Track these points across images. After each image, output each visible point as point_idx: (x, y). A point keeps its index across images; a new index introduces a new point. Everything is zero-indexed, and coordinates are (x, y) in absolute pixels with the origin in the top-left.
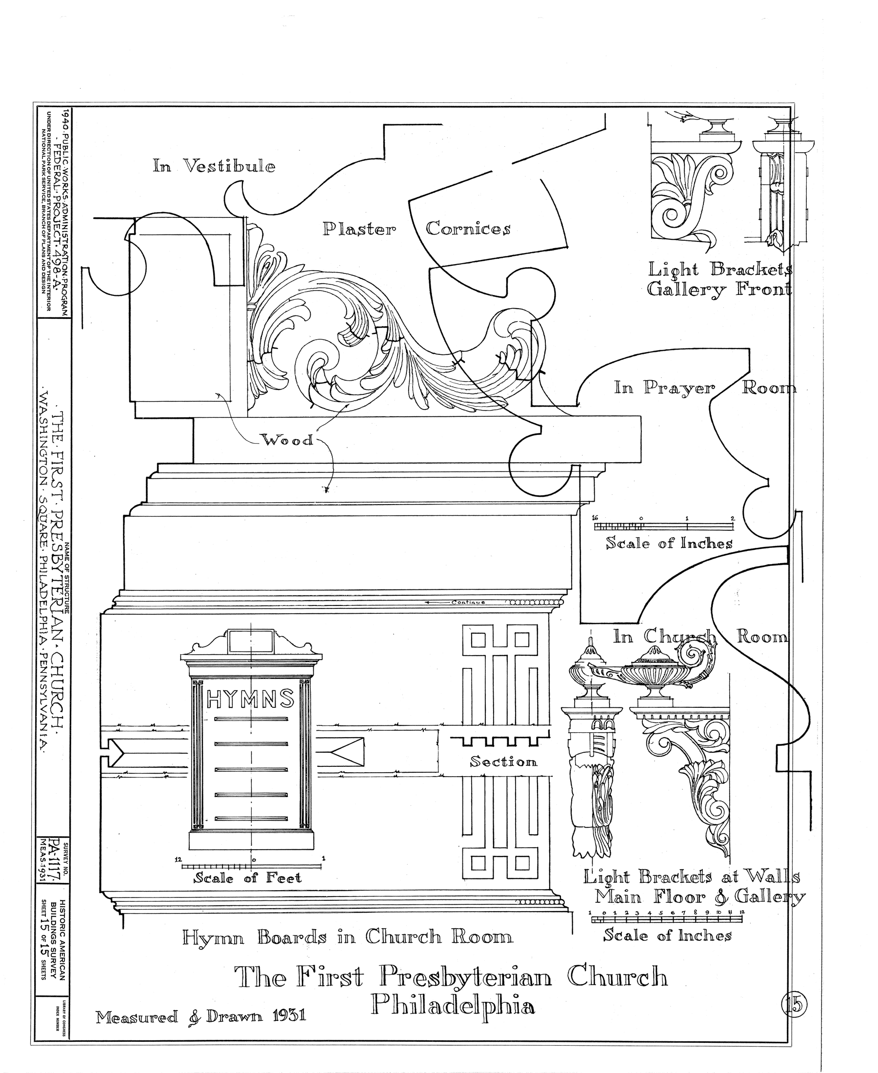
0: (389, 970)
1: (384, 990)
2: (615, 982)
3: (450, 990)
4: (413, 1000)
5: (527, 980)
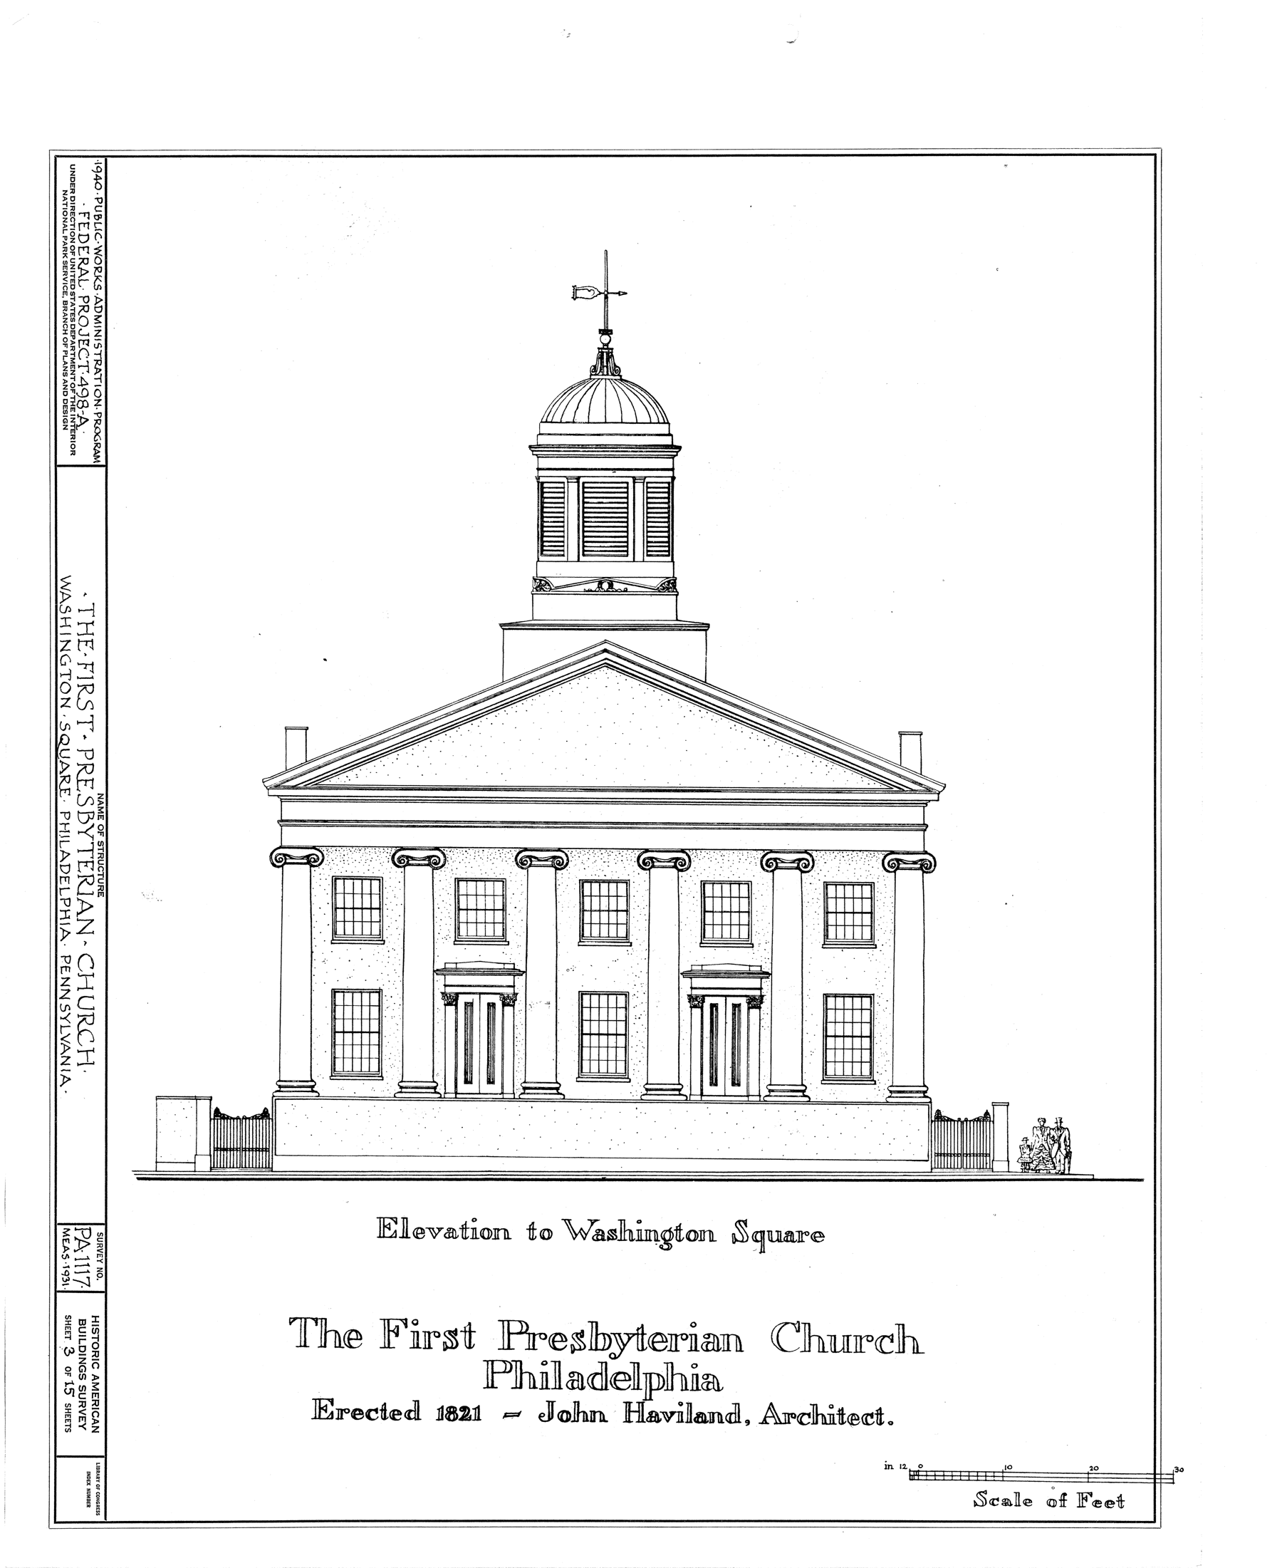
2: (839, 1347)
3: (604, 1356)
4: (544, 1369)
5: (714, 1343)
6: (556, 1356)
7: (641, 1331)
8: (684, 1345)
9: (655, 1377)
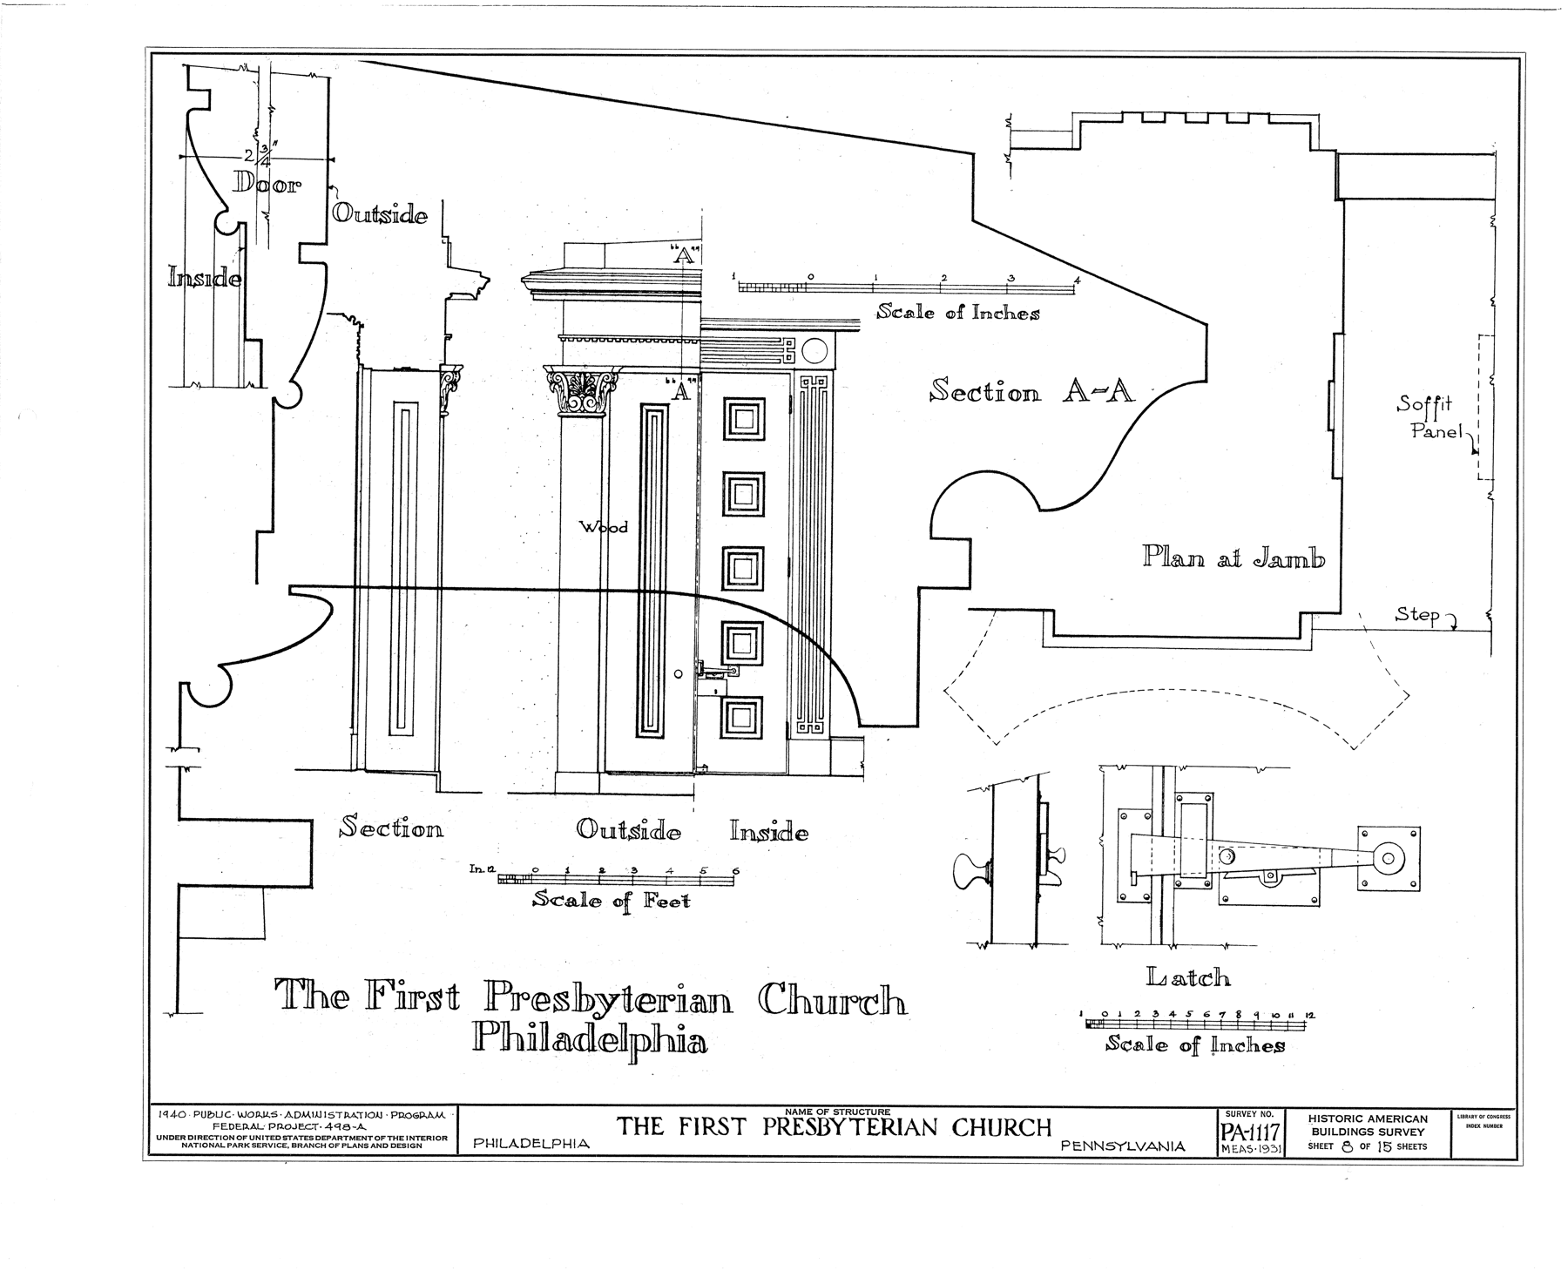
0: (499, 988)
1: (491, 1015)
3: (588, 1016)
5: (700, 1005)
6: (542, 1017)
7: (628, 992)
8: (672, 1006)
9: (640, 1039)
